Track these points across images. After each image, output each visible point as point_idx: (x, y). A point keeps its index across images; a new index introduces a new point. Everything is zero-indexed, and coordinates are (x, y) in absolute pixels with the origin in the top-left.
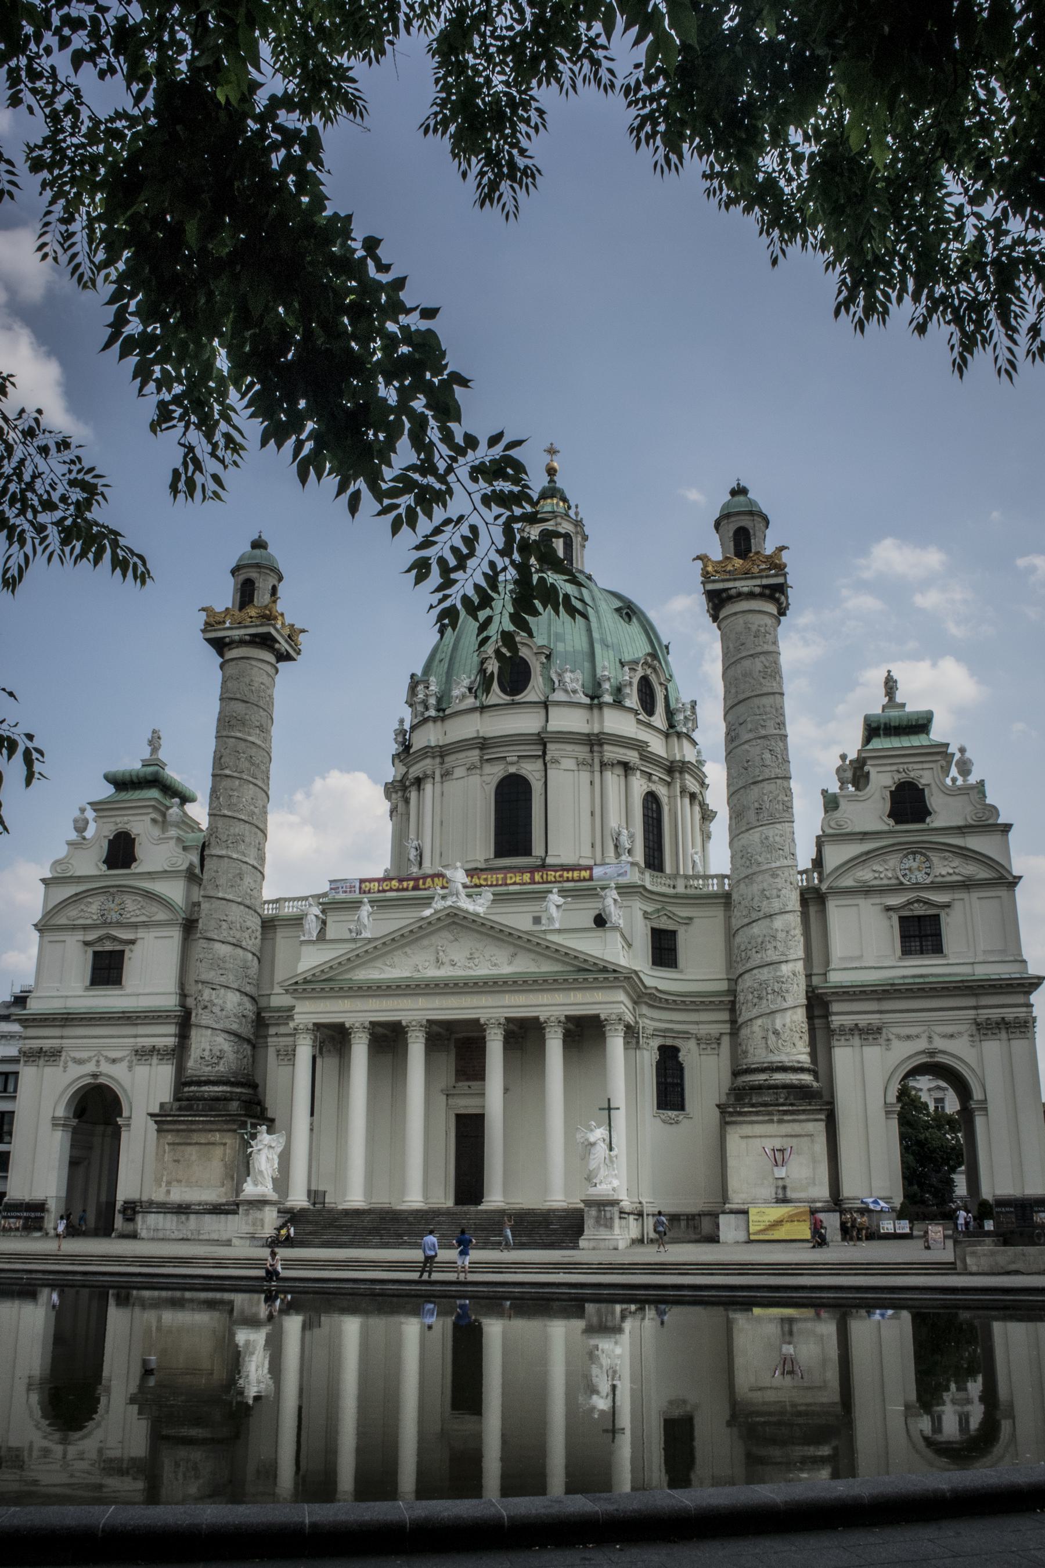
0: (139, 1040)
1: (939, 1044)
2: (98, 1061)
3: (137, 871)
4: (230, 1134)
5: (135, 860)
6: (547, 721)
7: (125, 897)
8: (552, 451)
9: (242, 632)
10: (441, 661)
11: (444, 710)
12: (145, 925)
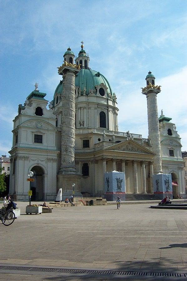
0: (48, 157)
1: (174, 170)
2: (38, 161)
3: (43, 117)
4: (79, 179)
5: (43, 114)
6: (108, 102)
7: (42, 122)
8: (82, 43)
9: (74, 70)
10: (83, 84)
11: (87, 95)
12: (48, 130)
